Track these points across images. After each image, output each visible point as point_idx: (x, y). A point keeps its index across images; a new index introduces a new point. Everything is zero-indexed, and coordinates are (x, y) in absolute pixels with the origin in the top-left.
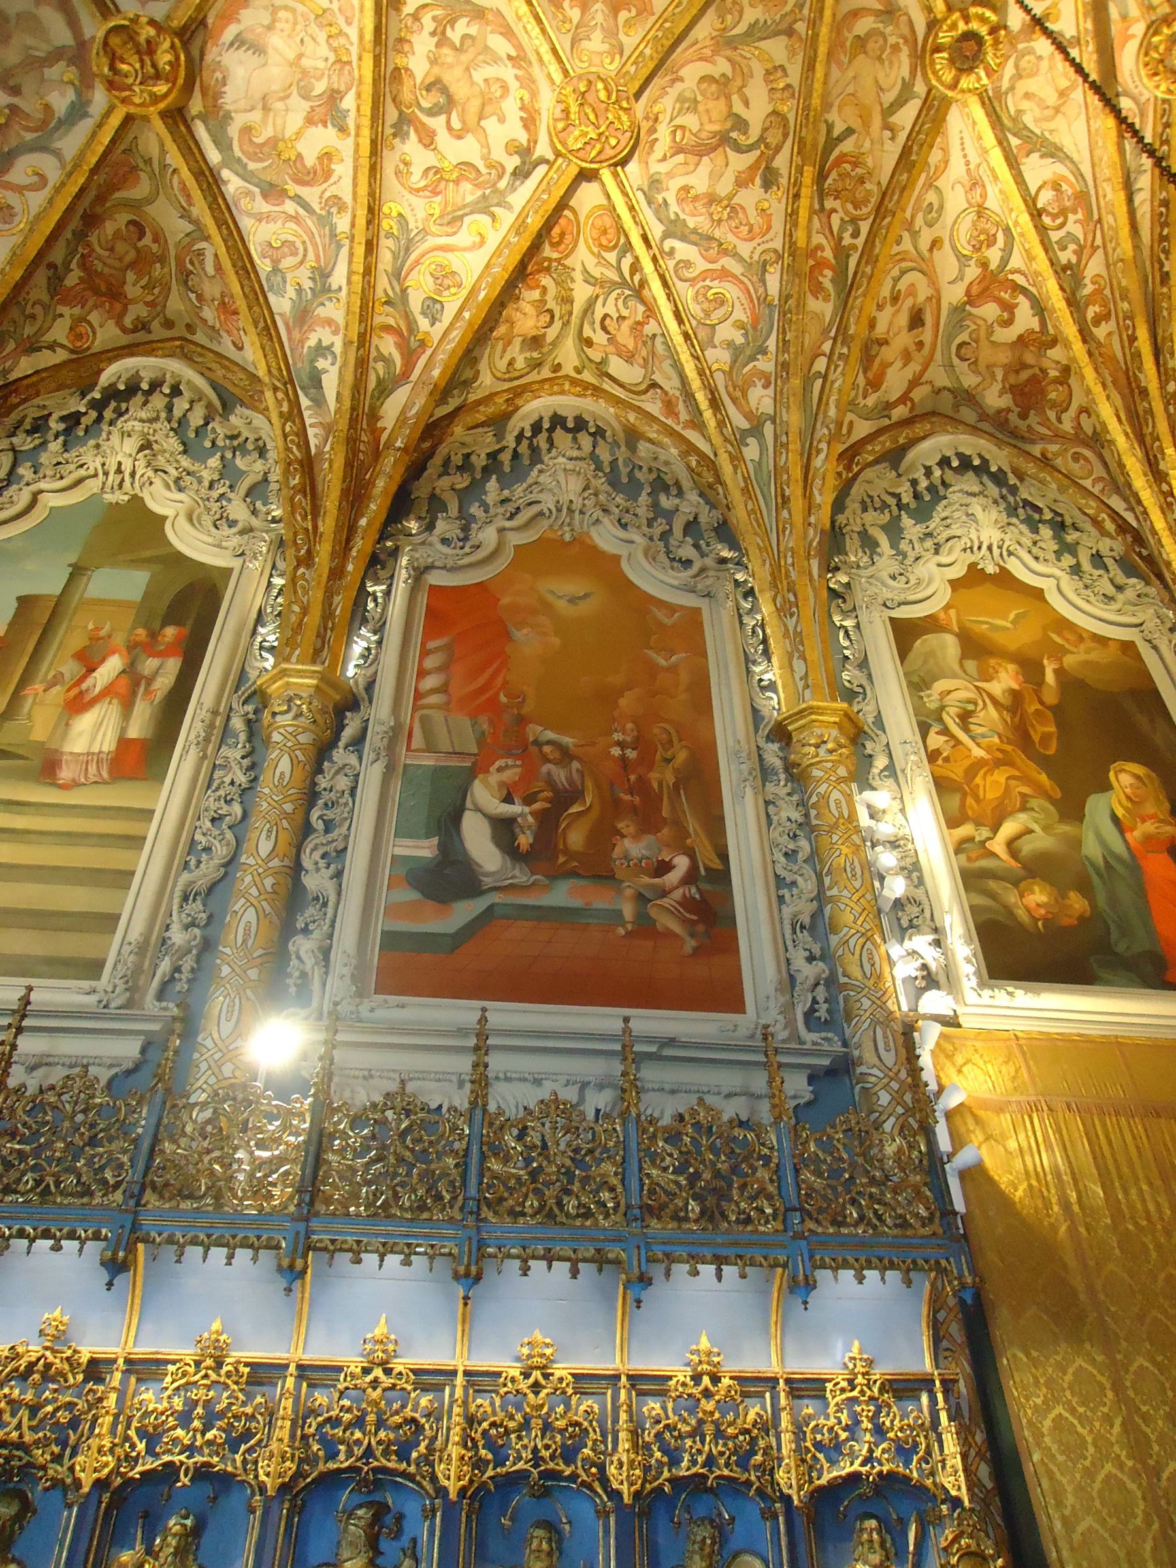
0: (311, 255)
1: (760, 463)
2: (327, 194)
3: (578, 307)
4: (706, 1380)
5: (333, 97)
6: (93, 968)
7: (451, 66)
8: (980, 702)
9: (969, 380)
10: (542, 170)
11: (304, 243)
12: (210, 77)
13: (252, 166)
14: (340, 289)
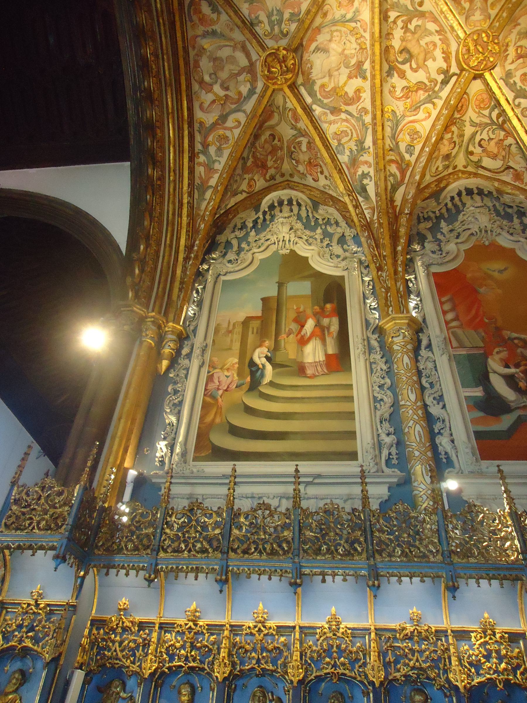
0: (355, 135)
2: (360, 107)
5: (360, 64)
6: (353, 456)
7: (410, 41)
10: (454, 79)
11: (351, 130)
12: (306, 67)
13: (325, 101)
14: (369, 147)
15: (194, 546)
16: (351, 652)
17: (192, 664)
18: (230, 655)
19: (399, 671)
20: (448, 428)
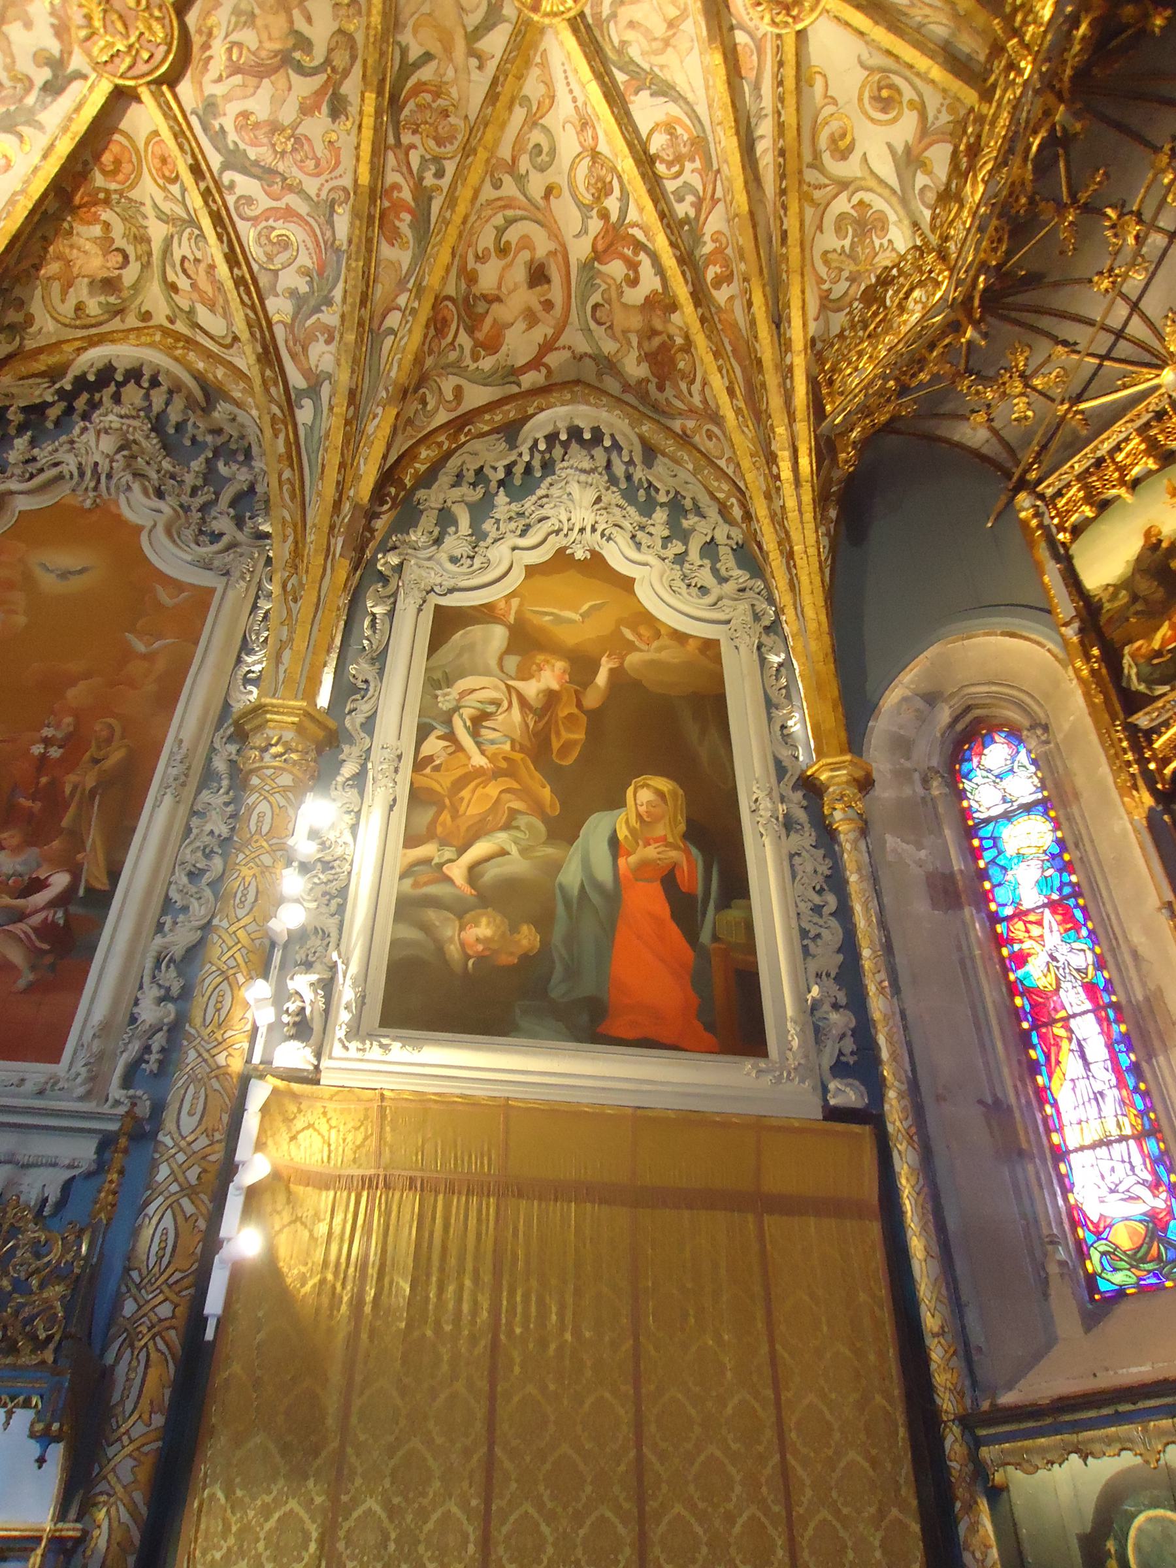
1: (311, 428)
3: (156, 247)
8: (505, 704)
9: (609, 347)
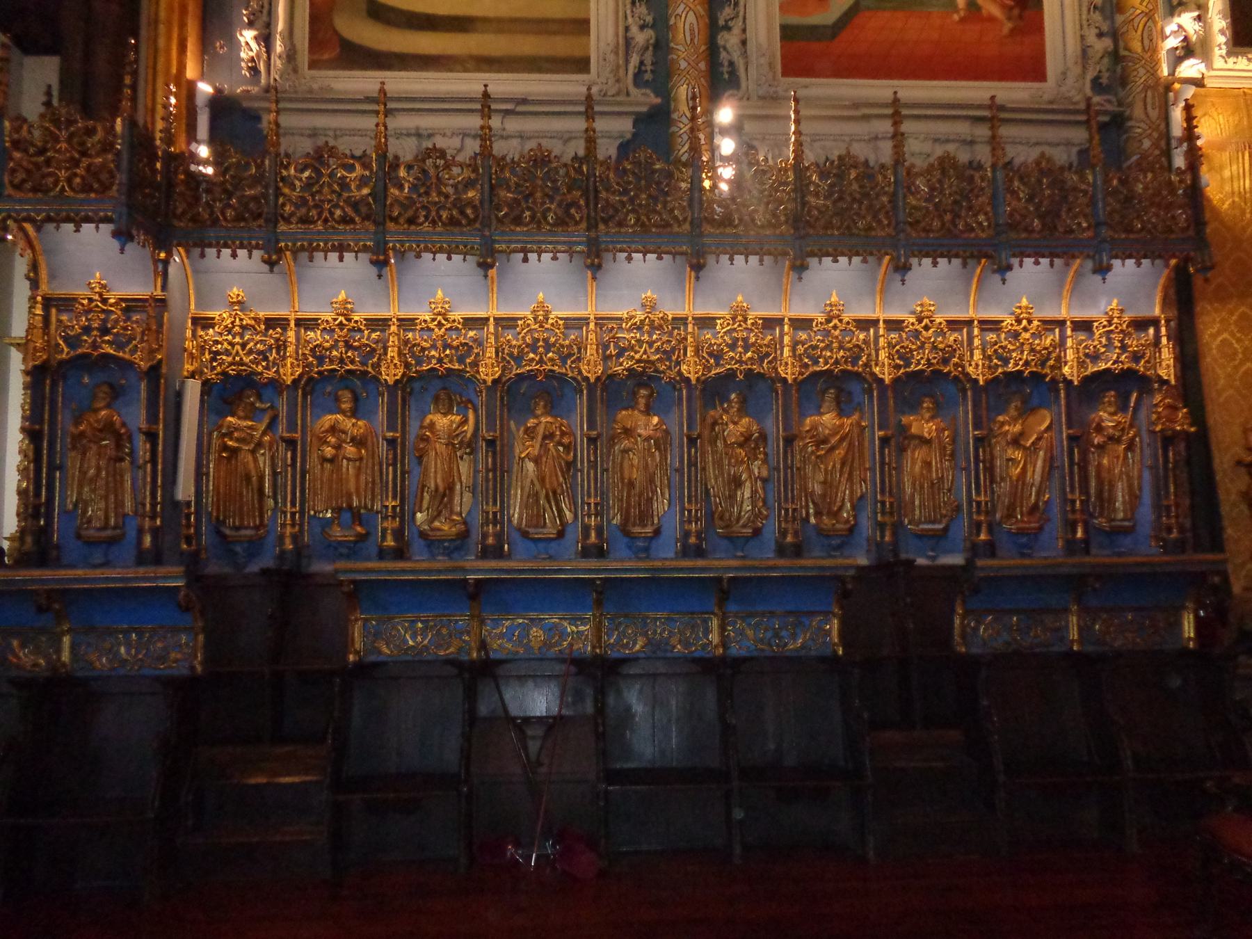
4: (1025, 322)
6: (581, 65)
15: (332, 214)
16: (562, 346)
17: (351, 367)
18: (400, 353)
19: (621, 364)
20: (741, 18)
